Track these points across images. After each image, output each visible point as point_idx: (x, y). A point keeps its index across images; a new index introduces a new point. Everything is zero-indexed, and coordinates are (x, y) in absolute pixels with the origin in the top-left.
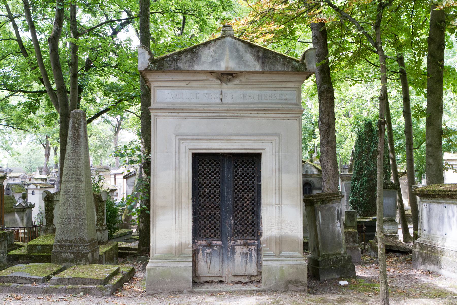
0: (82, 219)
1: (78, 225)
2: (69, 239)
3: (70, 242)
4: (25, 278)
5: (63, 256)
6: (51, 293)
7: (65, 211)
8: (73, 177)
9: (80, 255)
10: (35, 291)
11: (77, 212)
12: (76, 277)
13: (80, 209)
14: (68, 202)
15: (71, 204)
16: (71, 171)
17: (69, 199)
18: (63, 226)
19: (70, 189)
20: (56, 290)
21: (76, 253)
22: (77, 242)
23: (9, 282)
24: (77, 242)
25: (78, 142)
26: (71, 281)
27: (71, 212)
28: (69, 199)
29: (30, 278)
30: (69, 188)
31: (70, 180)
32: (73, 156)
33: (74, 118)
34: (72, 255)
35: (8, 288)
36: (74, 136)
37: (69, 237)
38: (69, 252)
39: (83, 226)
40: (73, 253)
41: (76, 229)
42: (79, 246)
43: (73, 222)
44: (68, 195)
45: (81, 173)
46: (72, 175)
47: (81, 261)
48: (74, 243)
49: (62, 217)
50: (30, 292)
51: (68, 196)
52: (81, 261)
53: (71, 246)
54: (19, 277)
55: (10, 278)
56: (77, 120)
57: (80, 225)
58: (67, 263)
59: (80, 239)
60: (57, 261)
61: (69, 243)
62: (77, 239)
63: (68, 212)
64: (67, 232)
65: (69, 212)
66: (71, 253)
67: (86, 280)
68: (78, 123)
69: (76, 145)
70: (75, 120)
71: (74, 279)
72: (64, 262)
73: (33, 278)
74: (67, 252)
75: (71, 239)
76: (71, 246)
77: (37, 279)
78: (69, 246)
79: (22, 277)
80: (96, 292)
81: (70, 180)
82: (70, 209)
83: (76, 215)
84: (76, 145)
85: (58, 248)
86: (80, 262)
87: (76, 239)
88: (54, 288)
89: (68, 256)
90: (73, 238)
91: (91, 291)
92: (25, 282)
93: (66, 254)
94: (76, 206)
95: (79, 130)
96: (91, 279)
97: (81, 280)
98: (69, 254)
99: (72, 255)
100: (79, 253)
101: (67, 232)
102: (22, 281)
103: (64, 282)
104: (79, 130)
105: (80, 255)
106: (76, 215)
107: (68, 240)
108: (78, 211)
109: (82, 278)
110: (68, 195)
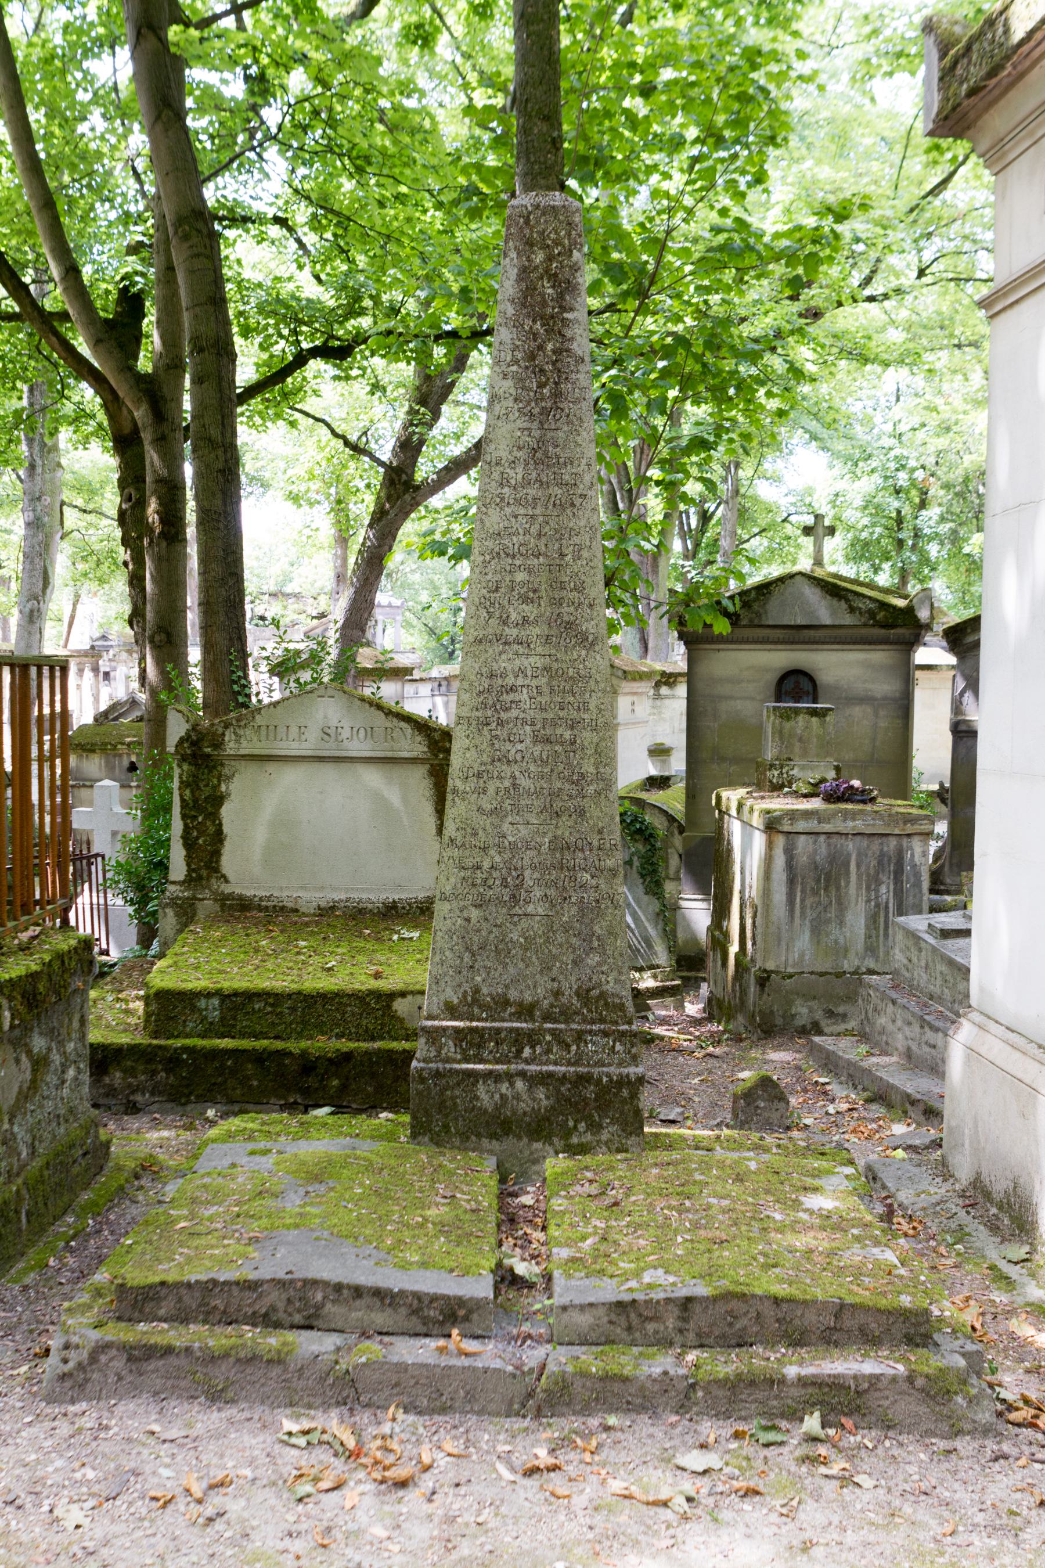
0: (598, 872)
1: (569, 913)
2: (513, 995)
3: (526, 1011)
4: (379, 1294)
5: (485, 1096)
6: (586, 1410)
7: (486, 822)
8: (527, 609)
9: (590, 1092)
10: (470, 1397)
11: (565, 828)
12: (743, 1297)
13: (582, 813)
14: (507, 770)
15: (525, 783)
16: (521, 576)
17: (512, 750)
18: (474, 914)
19: (513, 689)
20: (616, 1387)
21: (564, 1079)
22: (566, 1015)
23: (268, 1321)
24: (566, 1015)
25: (557, 395)
26: (700, 1319)
27: (524, 831)
28: (512, 750)
29: (417, 1296)
30: (510, 681)
31: (512, 632)
32: (526, 483)
33: (530, 243)
34: (541, 1093)
35: (275, 1371)
36: (532, 357)
37: (515, 981)
38: (522, 1074)
39: (600, 914)
40: (544, 1079)
41: (560, 938)
42: (580, 1036)
43: (538, 893)
44: (501, 723)
45: (580, 589)
46: (525, 600)
47: (595, 1127)
48: (547, 1017)
49: (469, 862)
50: (436, 1397)
51: (502, 733)
52: (595, 1127)
53: (532, 1038)
54: (338, 1287)
55: (275, 1297)
56: (550, 259)
57: (583, 908)
58: (511, 1140)
59: (583, 994)
60: (446, 1127)
61: (518, 1016)
62: (569, 998)
63: (506, 827)
64: (502, 951)
65: (515, 831)
66: (535, 1081)
67: (811, 1317)
68: (553, 277)
69: (545, 412)
70: (539, 257)
71: (721, 1308)
72: (493, 1136)
73: (434, 1298)
74: (509, 1077)
75: (528, 997)
76: (532, 1038)
77: (460, 1302)
78: (519, 1039)
79: (358, 1291)
80: (905, 1407)
81: (512, 632)
82: (516, 809)
83: (560, 846)
84: (545, 412)
85: (450, 1048)
86: (589, 1137)
87: (557, 994)
88: (607, 1378)
89: (517, 1097)
90: (537, 990)
91: (872, 1400)
92: (381, 1318)
93: (504, 1088)
94: (555, 794)
95: (565, 322)
96: (841, 1309)
97: (769, 1311)
98: (520, 1084)
99: (541, 1093)
100: (584, 1079)
101: (502, 951)
102: (358, 1313)
103: (651, 1327)
104: (565, 322)
105: (590, 1092)
106: (560, 846)
107: (507, 1003)
108: (566, 821)
109: (777, 1301)
110: (501, 723)
